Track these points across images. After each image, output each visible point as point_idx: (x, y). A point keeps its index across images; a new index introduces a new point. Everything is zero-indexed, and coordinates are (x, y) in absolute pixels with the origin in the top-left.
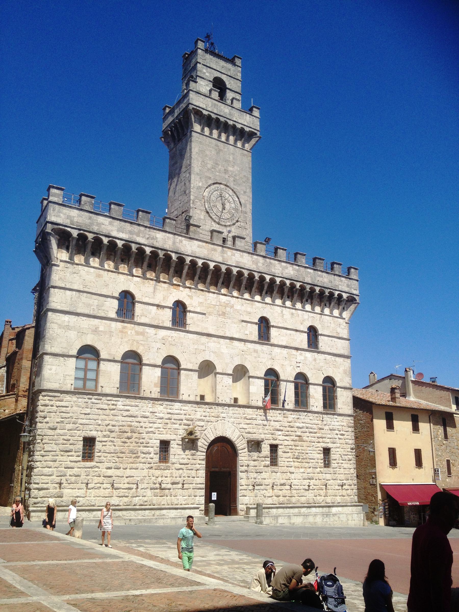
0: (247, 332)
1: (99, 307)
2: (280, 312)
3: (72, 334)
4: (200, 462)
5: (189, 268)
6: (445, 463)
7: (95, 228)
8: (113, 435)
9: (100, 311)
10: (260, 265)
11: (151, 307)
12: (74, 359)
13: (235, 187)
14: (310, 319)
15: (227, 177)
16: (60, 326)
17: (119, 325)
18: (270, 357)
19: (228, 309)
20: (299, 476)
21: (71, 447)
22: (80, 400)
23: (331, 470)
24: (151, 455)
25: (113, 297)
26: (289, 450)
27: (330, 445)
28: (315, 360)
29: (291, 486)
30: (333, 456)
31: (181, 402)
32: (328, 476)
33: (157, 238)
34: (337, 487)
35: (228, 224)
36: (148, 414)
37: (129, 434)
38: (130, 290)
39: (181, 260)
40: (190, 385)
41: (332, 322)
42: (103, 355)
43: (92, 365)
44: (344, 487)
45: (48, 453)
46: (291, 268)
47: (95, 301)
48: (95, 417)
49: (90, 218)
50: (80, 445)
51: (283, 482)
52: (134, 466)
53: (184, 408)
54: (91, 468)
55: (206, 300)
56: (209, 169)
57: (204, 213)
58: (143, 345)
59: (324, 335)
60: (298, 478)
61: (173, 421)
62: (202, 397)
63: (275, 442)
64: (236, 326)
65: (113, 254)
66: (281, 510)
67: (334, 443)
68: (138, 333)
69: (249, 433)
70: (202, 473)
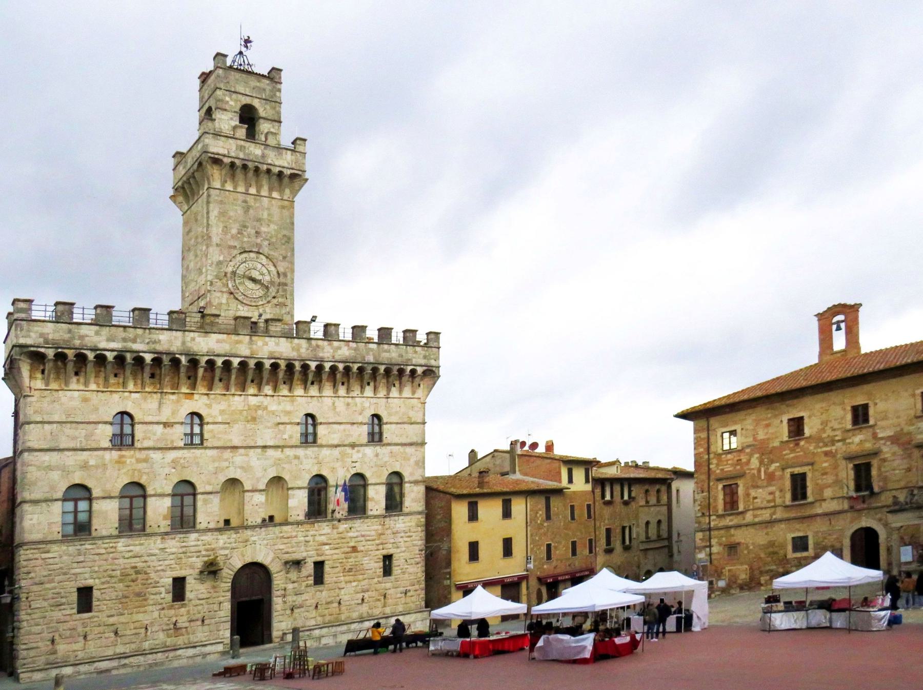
0: (286, 436)
1: (87, 437)
2: (331, 404)
3: (55, 475)
4: (223, 594)
5: (206, 370)
6: (544, 548)
7: (77, 343)
8: (113, 580)
9: (89, 442)
10: (303, 350)
11: (156, 426)
12: (60, 503)
13: (271, 253)
14: (372, 407)
15: (259, 241)
16: (39, 468)
17: (115, 454)
18: (315, 461)
19: (260, 412)
20: (352, 590)
21: (64, 600)
22: (70, 548)
23: (392, 578)
24: (162, 596)
25: (106, 423)
26: (338, 565)
27: (391, 551)
28: (377, 455)
29: (340, 603)
30: (395, 562)
31: (198, 531)
32: (388, 585)
33: (160, 341)
34: (399, 595)
35: (261, 303)
36: (157, 551)
37: (134, 576)
38: (128, 410)
39: (194, 362)
40: (209, 511)
41: (402, 406)
42: (96, 493)
43: (83, 505)
44: (409, 594)
45: (35, 611)
46: (346, 348)
47: (81, 432)
48: (90, 564)
49: (70, 331)
50: (74, 597)
51: (329, 600)
52: (142, 609)
53: (202, 538)
54: (89, 618)
55: (229, 406)
56: (232, 237)
57: (225, 296)
58: (148, 474)
59: (391, 423)
60: (349, 593)
61: (189, 554)
62: (227, 522)
63: (320, 559)
64: (270, 430)
65: (103, 369)
66: (325, 631)
67: (398, 547)
68: (139, 461)
69: (287, 553)
70: (227, 606)
